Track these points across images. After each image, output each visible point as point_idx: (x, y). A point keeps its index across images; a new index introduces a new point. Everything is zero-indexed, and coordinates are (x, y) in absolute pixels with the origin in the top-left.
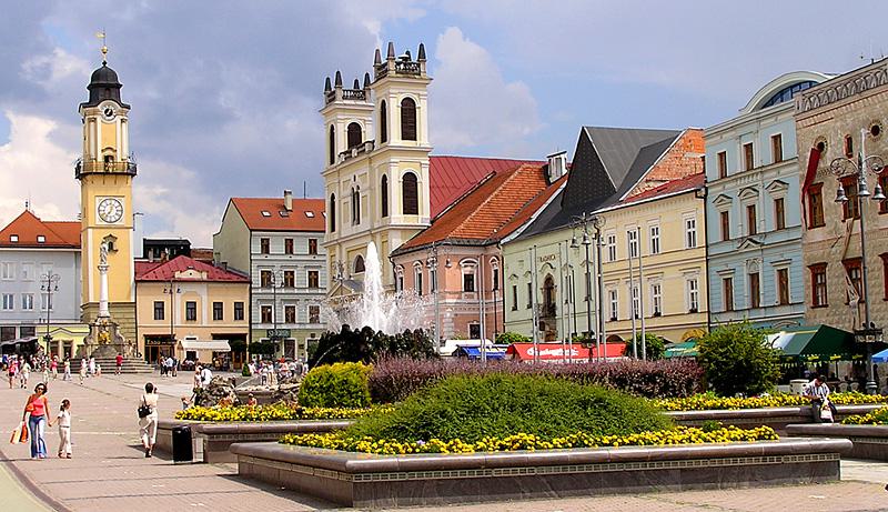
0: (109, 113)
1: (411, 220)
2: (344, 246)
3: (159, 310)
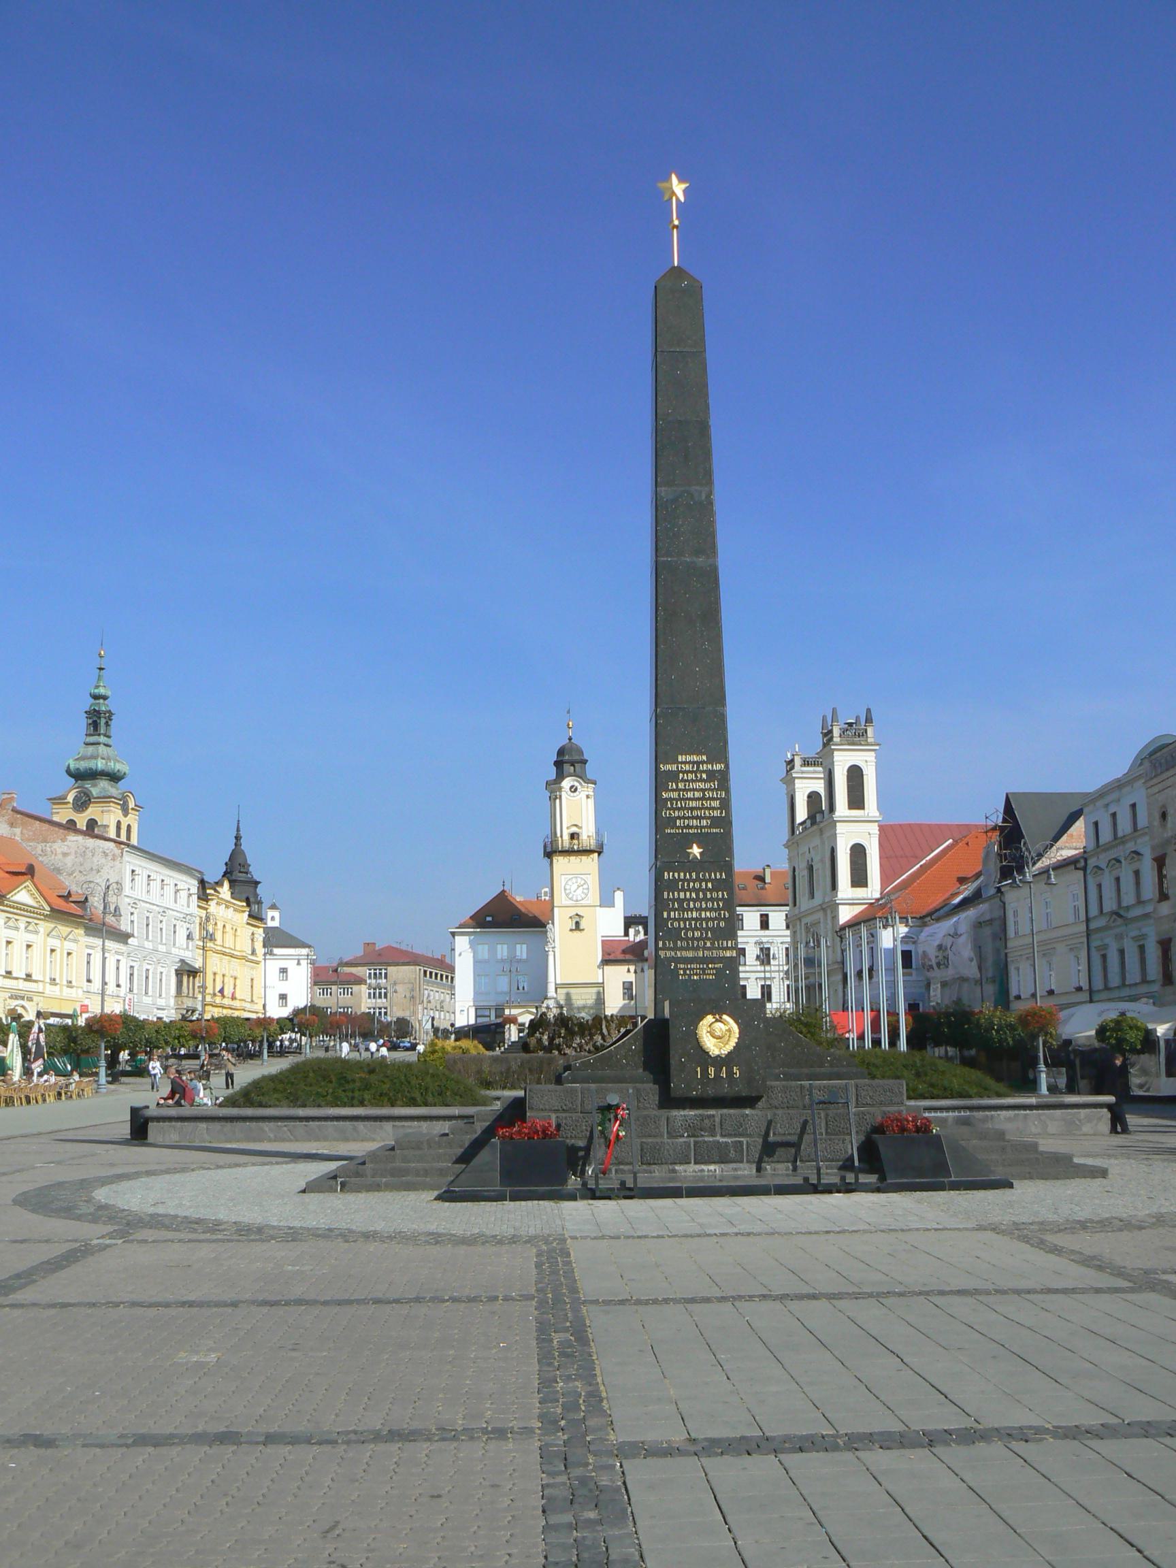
0: (573, 789)
1: (860, 892)
2: (804, 921)
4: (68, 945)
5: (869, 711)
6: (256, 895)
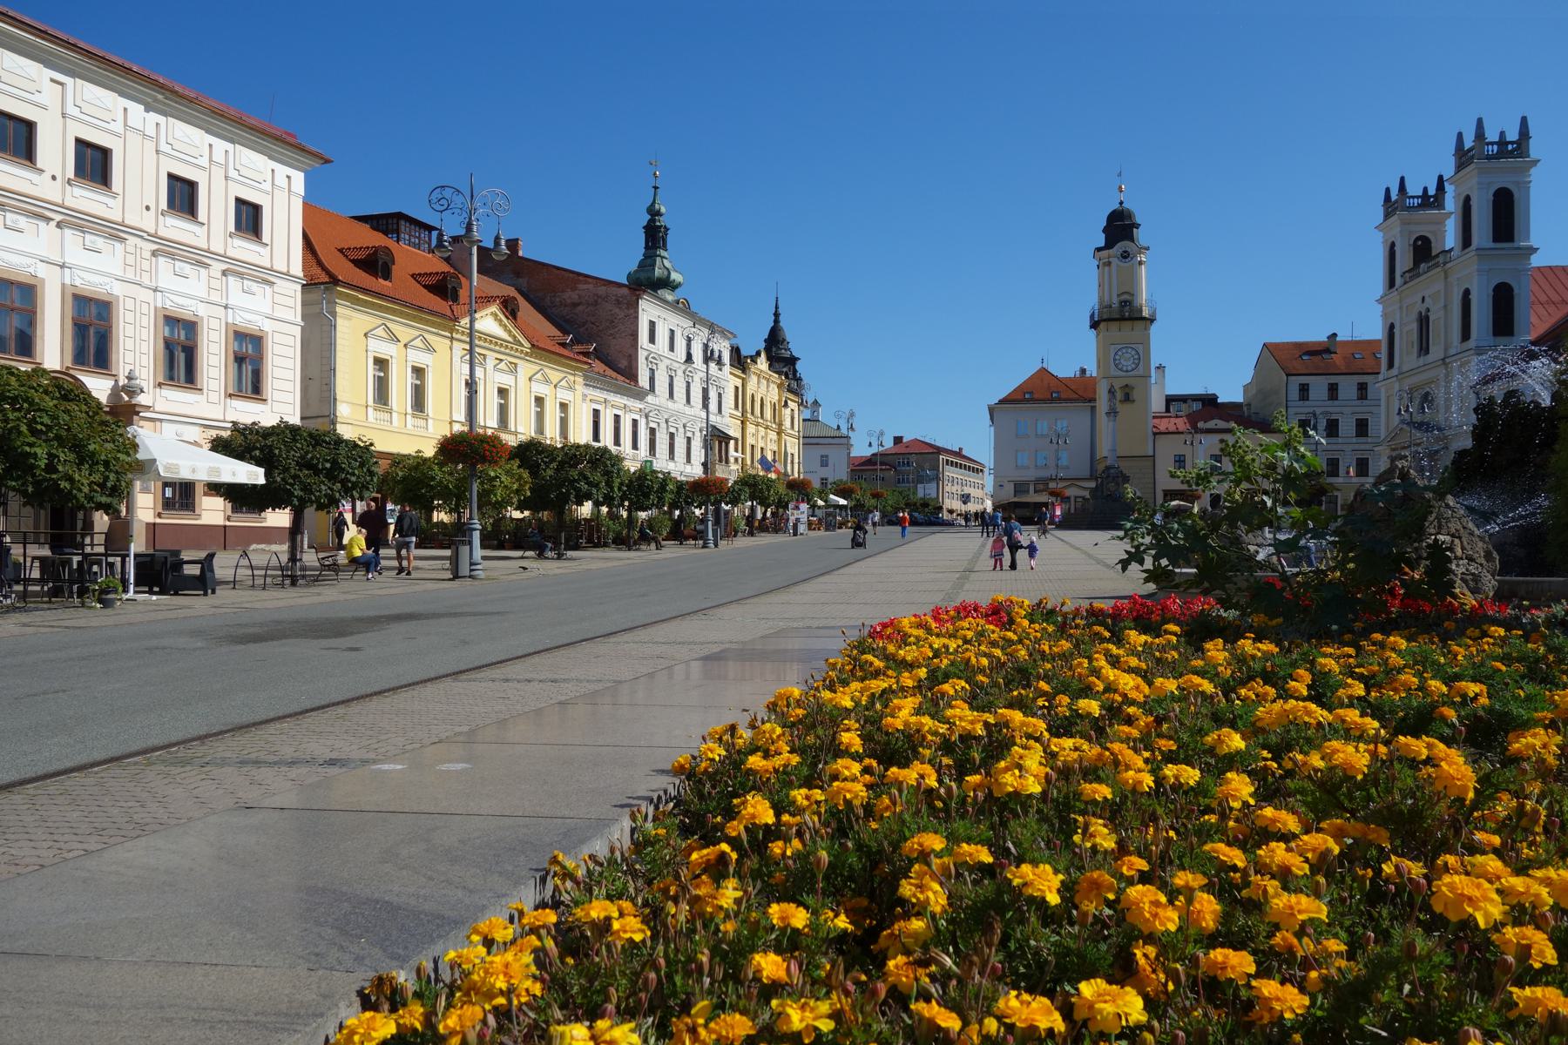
0: (1125, 255)
5: (1524, 121)
6: (795, 371)
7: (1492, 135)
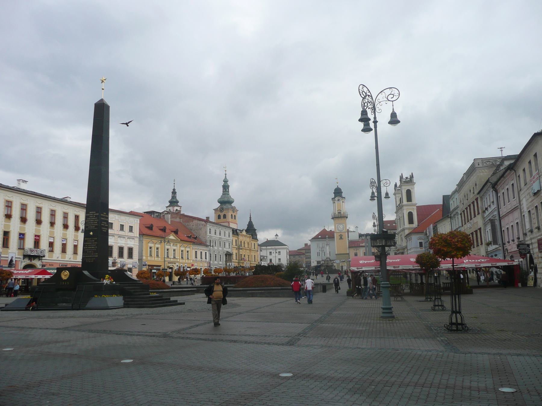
0: (338, 200)
1: (411, 226)
3: (356, 255)
4: (188, 249)
7: (404, 177)
